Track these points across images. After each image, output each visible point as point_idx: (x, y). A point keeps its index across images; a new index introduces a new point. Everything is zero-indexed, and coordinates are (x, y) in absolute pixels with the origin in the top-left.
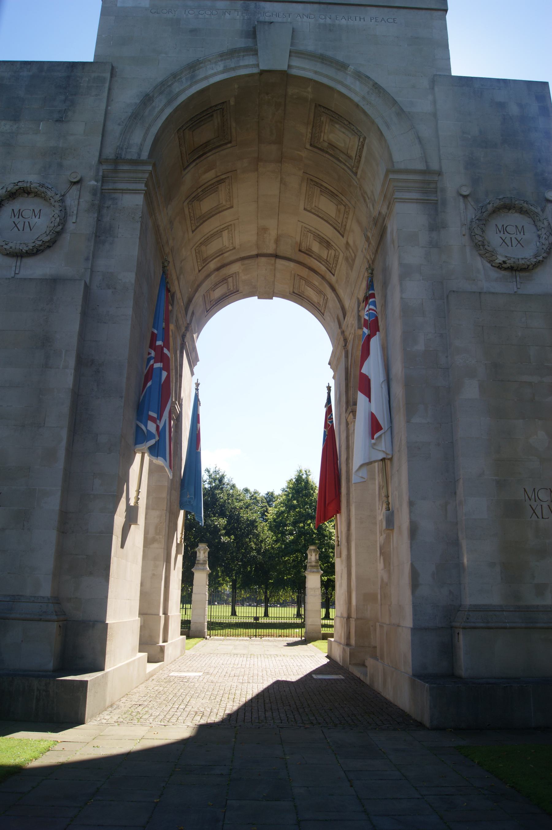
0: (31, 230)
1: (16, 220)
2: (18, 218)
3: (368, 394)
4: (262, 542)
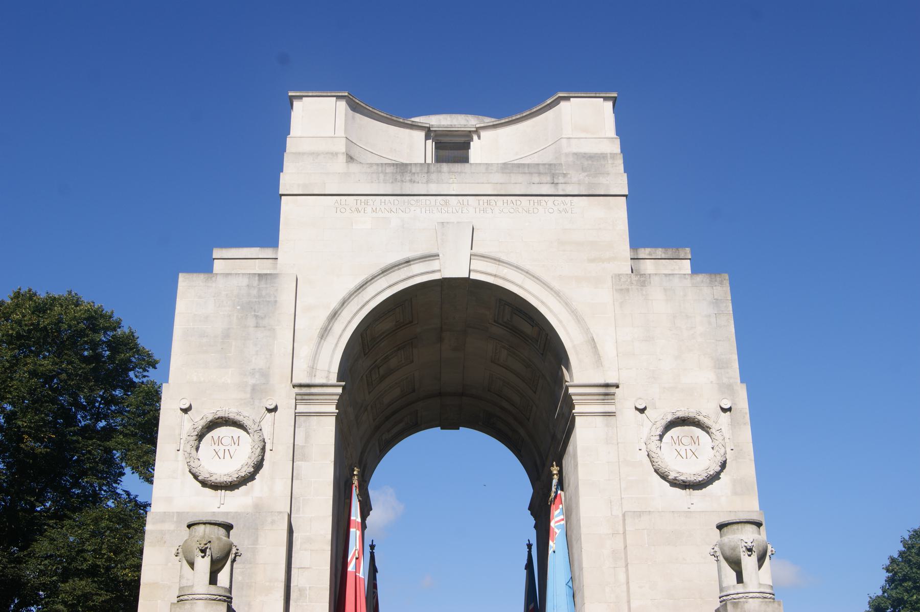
0: (231, 458)
1: (217, 448)
2: (218, 445)
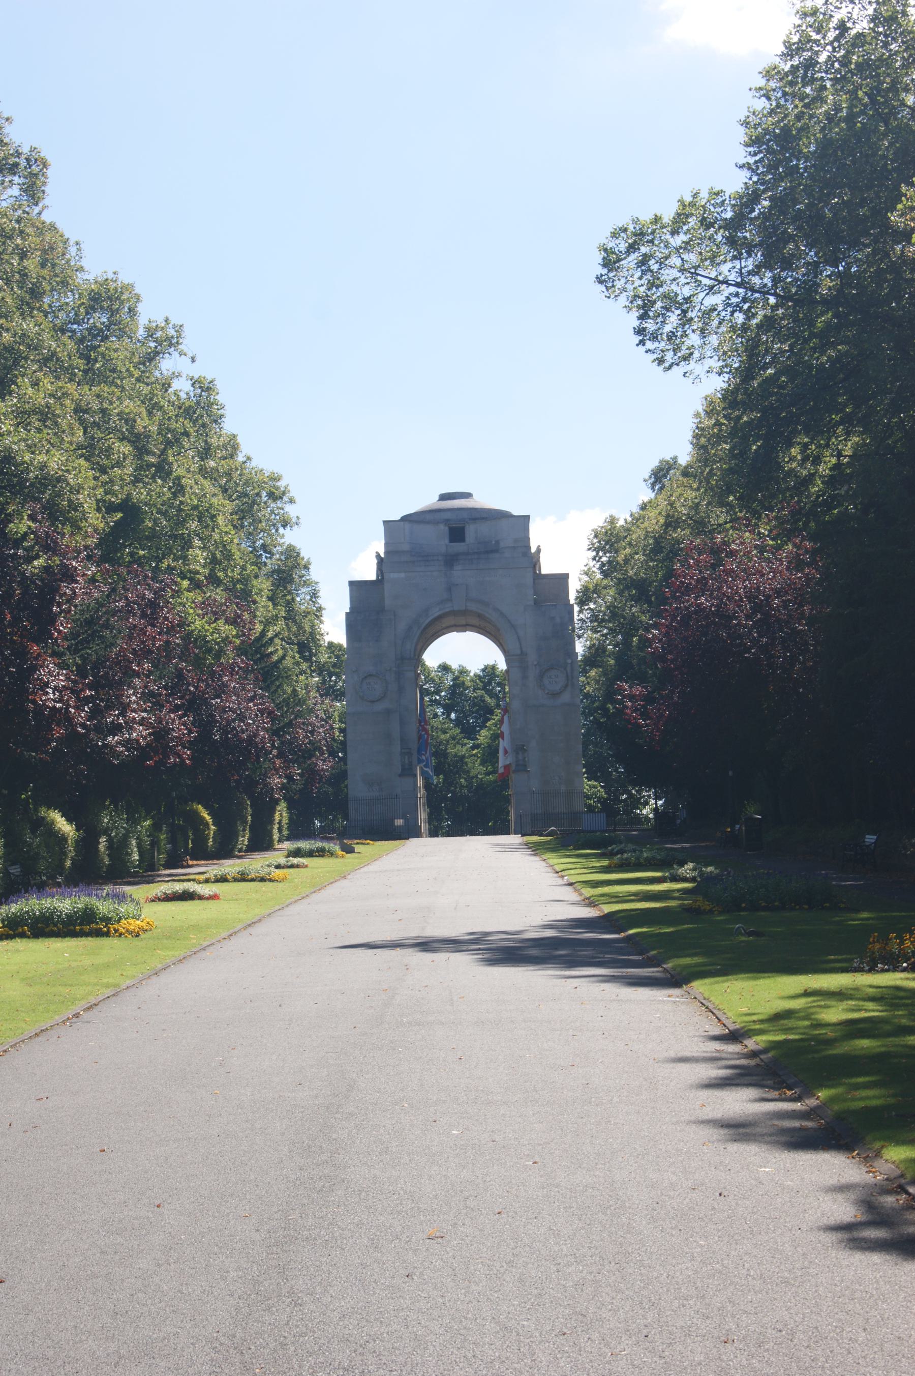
3: (503, 739)
4: (473, 778)
